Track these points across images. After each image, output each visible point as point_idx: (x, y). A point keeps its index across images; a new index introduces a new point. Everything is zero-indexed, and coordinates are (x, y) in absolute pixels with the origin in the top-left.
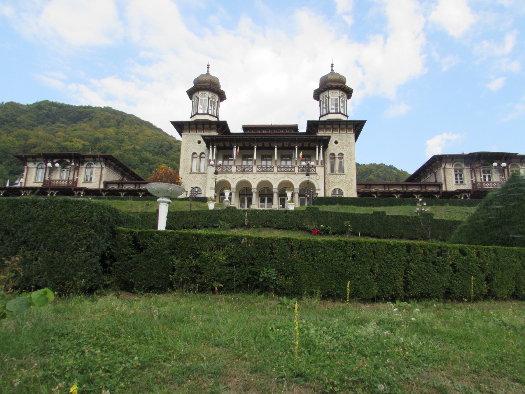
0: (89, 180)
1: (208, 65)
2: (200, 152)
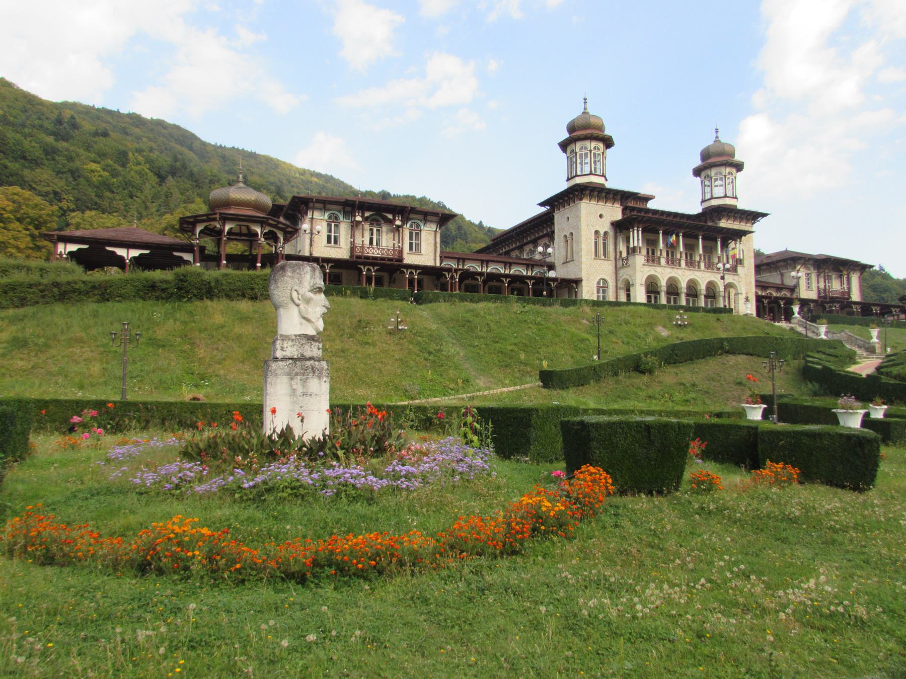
0: (415, 248)
1: (585, 99)
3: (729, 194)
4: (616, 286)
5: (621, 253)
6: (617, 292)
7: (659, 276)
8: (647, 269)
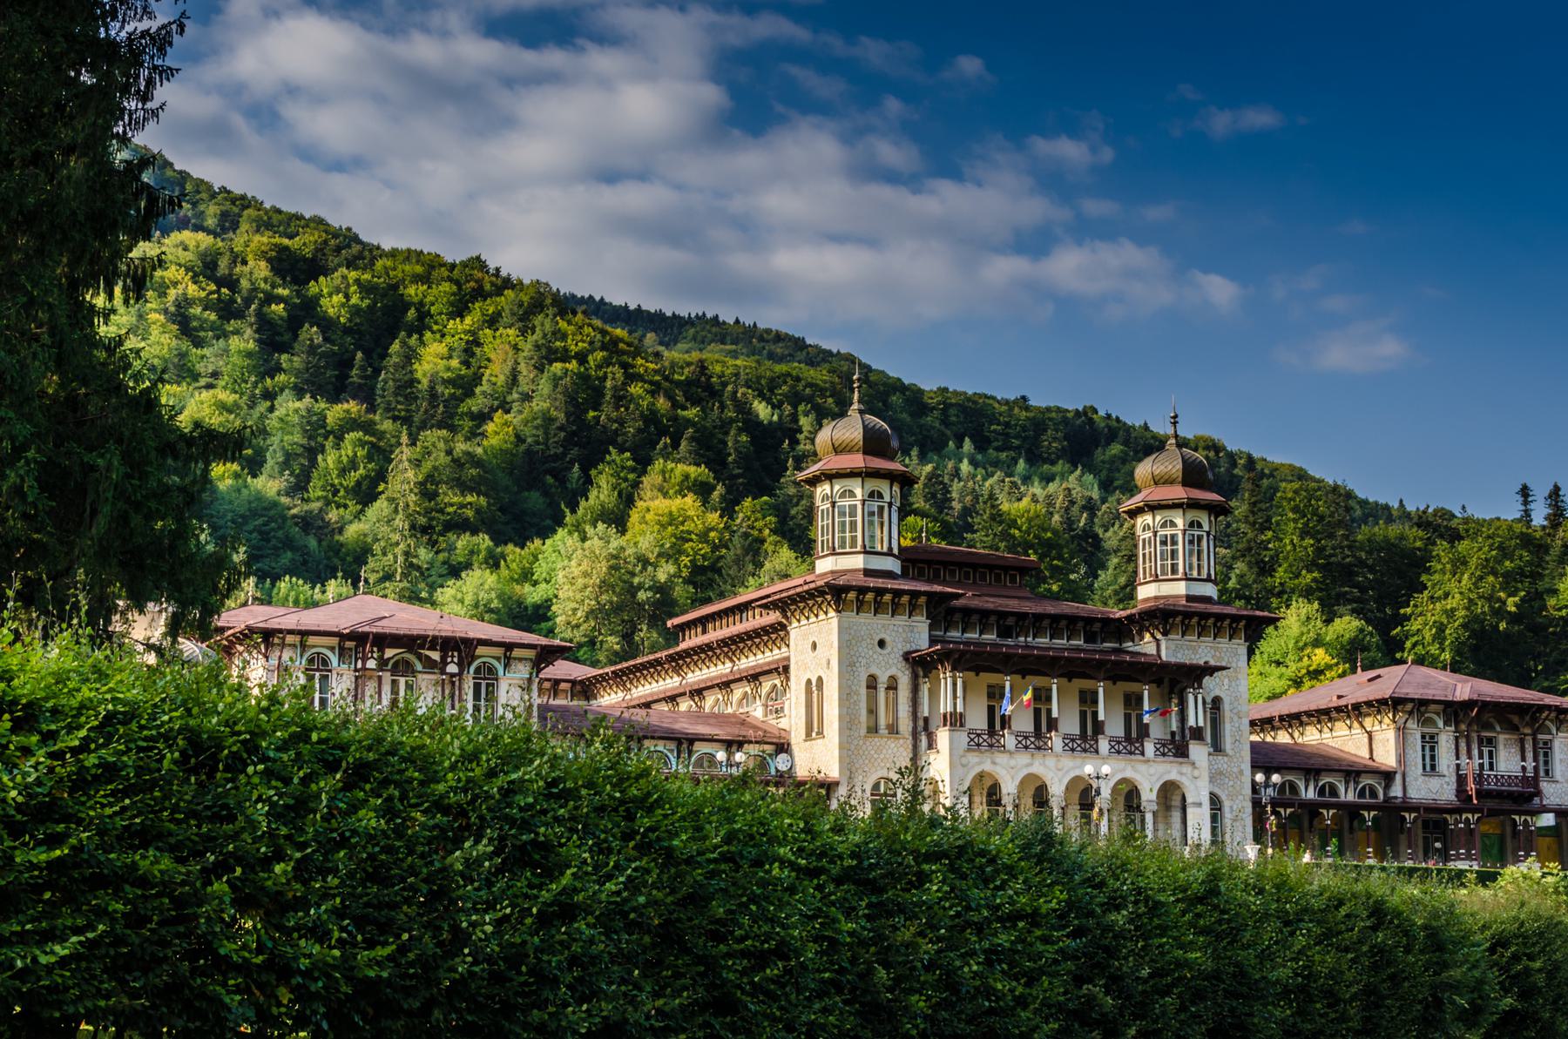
2: (889, 673)
8: (973, 758)
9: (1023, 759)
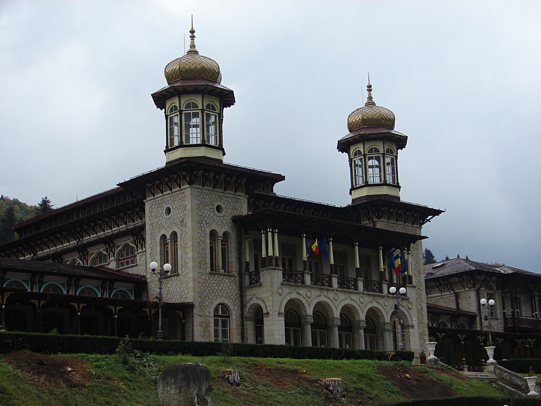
1: (192, 32)
2: (223, 230)
3: (389, 180)
4: (242, 315)
5: (247, 264)
6: (242, 325)
7: (304, 301)
8: (286, 290)
9: (315, 293)
